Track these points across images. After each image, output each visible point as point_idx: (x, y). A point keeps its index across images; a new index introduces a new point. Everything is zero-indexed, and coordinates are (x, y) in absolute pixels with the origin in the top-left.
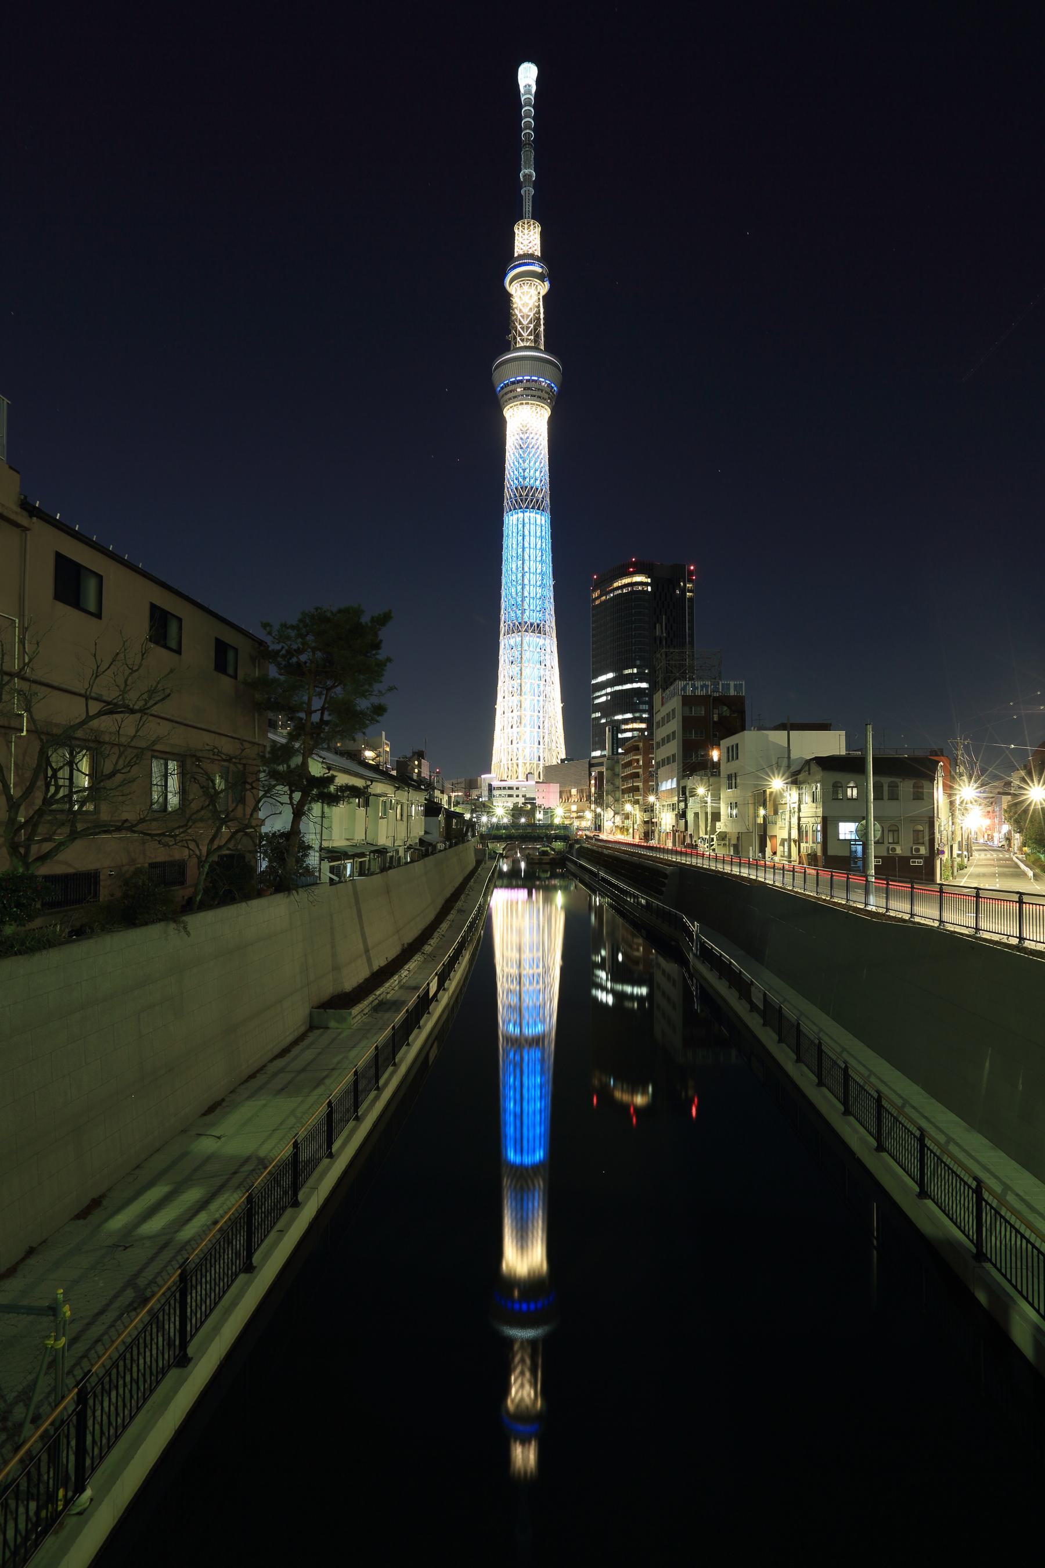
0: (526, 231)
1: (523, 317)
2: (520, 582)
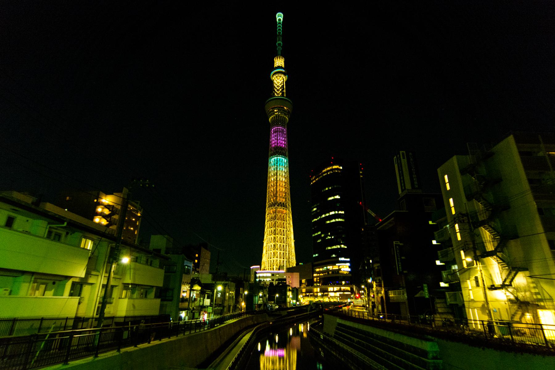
0: (279, 59)
1: (277, 87)
2: (275, 185)
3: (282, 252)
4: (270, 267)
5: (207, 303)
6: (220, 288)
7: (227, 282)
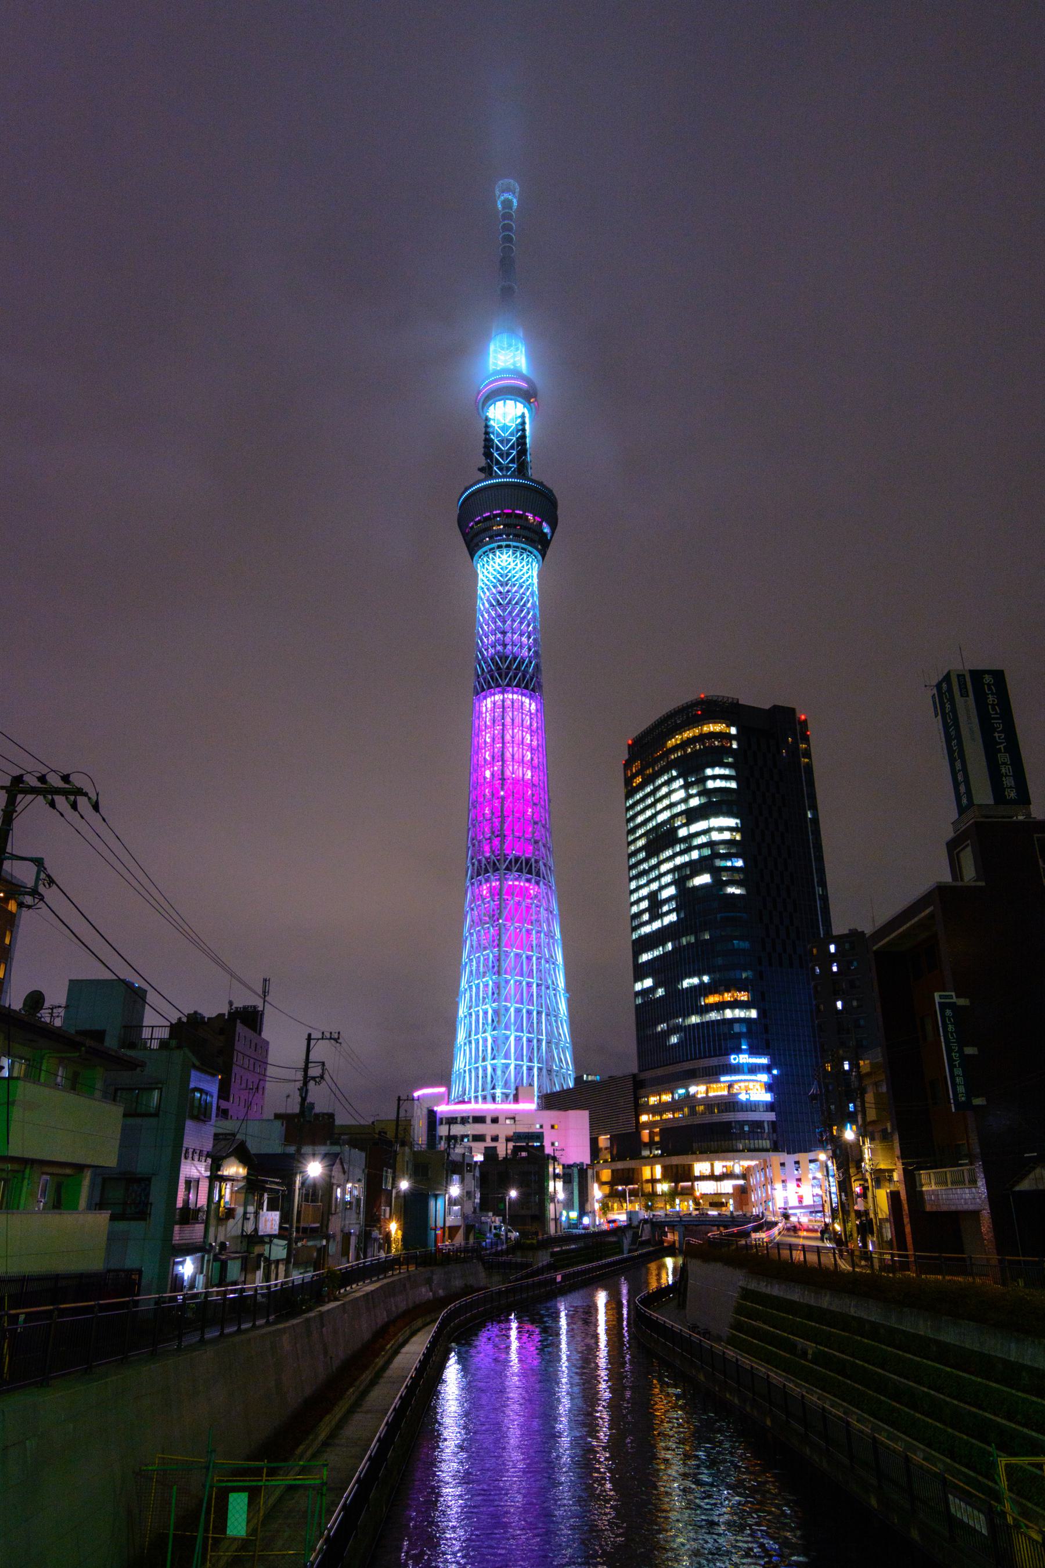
1: (501, 442)
3: (525, 1036)
4: (483, 1090)
5: (269, 1224)
6: (314, 1169)
7: (336, 1149)
